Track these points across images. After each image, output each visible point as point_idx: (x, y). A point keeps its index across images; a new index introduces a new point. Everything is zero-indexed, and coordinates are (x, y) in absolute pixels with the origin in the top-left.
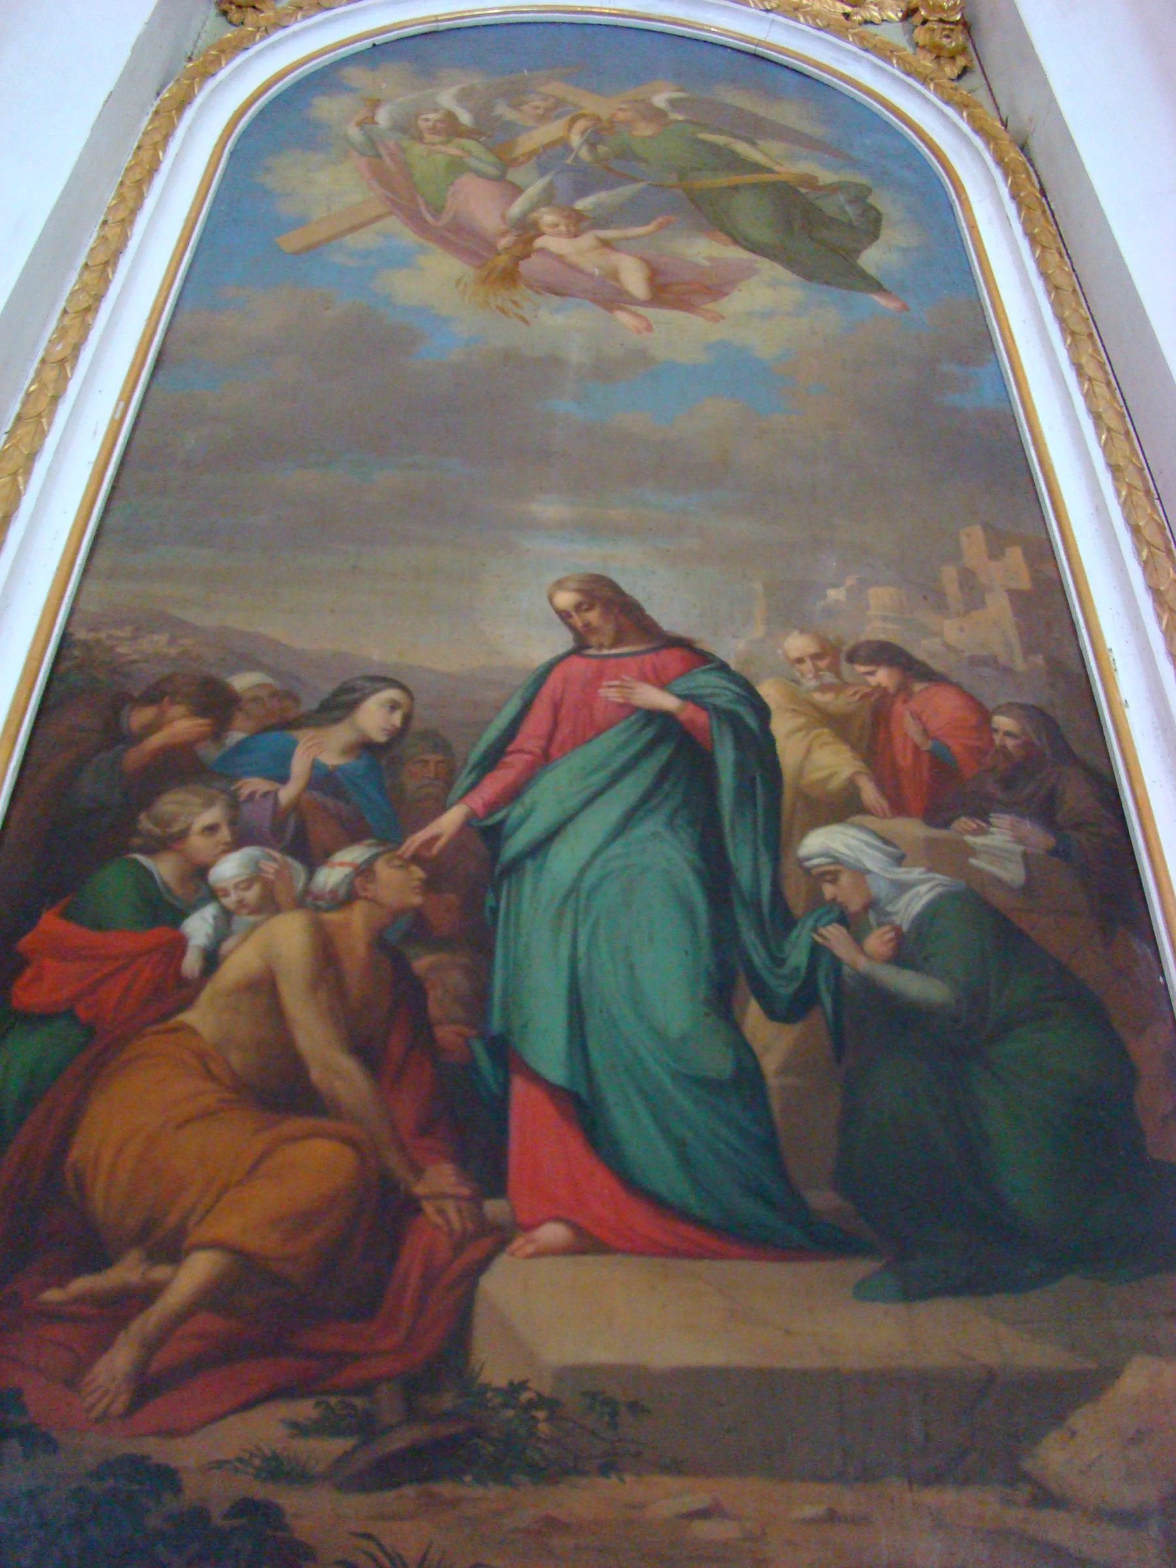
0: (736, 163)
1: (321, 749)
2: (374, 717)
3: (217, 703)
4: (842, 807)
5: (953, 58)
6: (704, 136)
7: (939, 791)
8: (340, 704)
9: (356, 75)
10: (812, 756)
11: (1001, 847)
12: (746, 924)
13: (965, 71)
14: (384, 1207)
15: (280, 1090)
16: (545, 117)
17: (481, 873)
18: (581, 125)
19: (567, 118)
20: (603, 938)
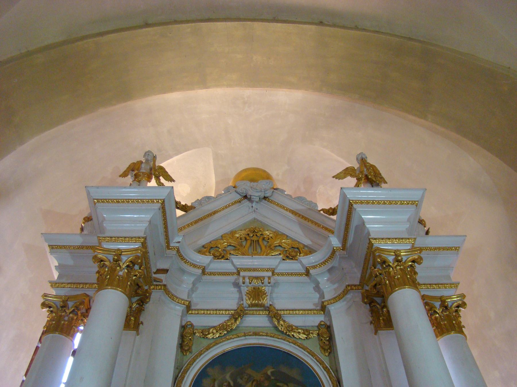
5: (327, 350)
6: (278, 384)
9: (209, 370)
13: (330, 353)
16: (247, 382)
18: (254, 383)
19: (251, 382)
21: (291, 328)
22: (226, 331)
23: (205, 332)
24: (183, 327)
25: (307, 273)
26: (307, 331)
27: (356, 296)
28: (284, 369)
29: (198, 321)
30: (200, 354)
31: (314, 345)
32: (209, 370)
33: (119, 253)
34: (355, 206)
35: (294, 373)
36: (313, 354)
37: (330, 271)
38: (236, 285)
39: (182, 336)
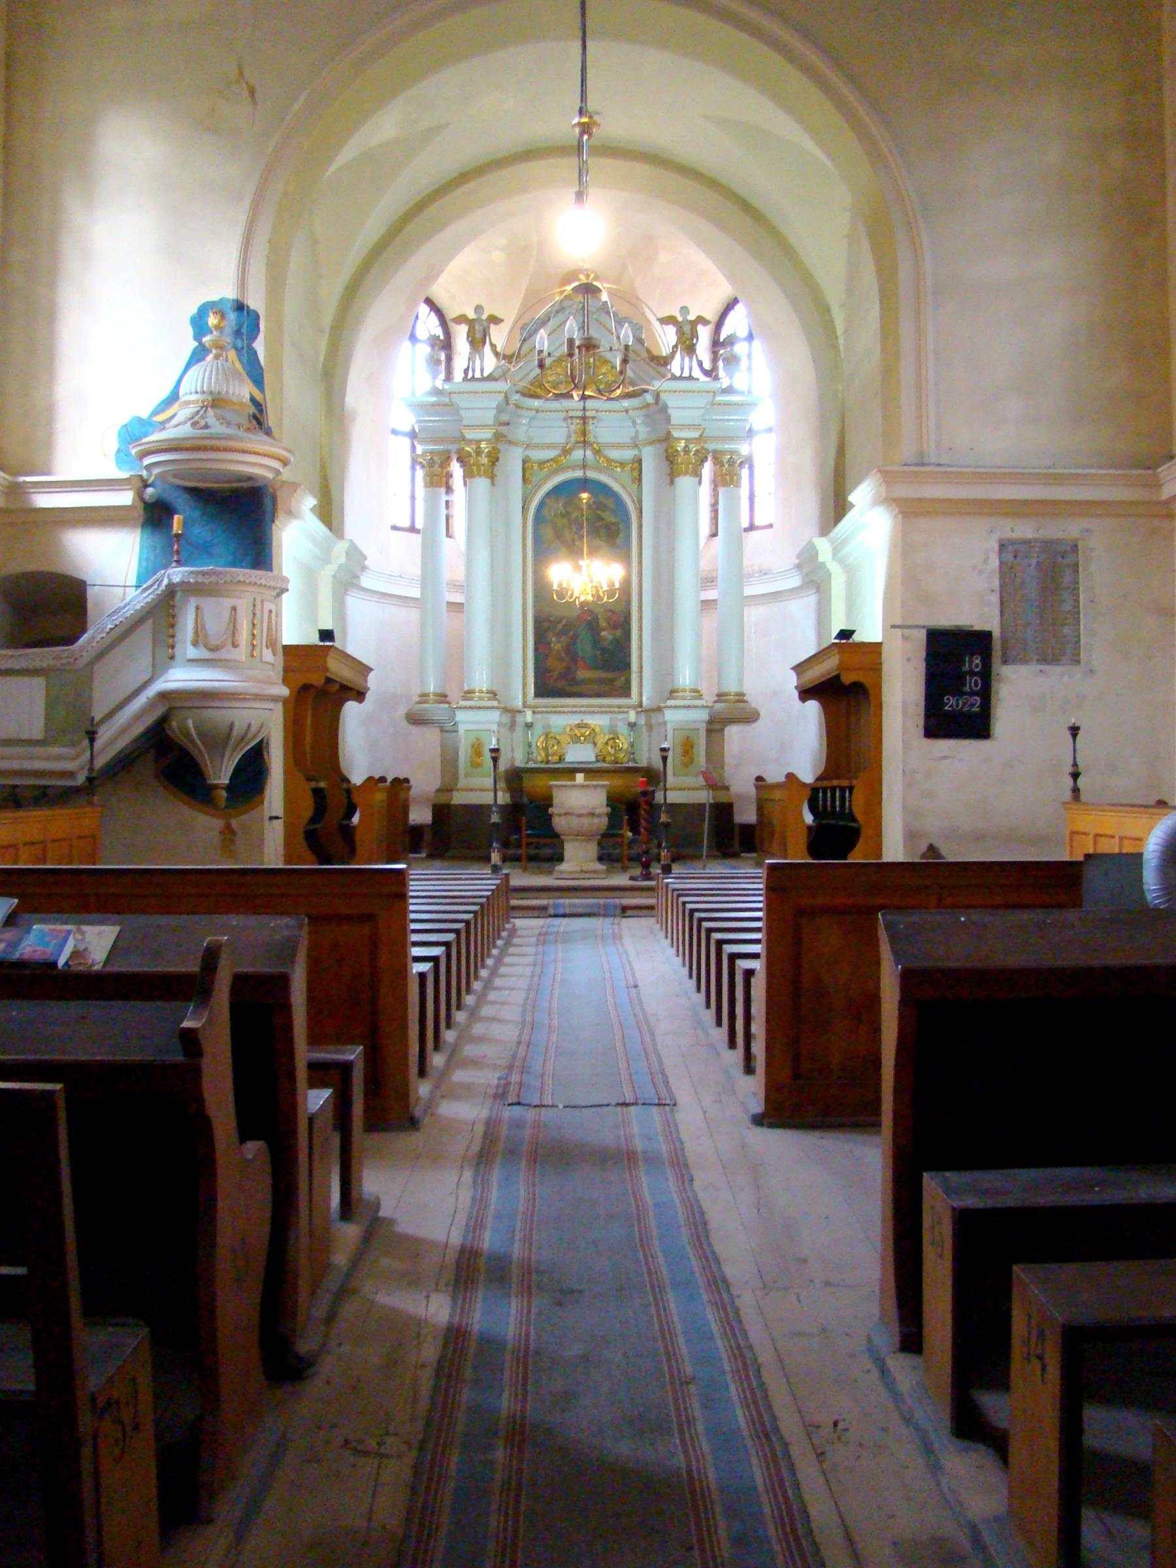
0: (602, 519)
1: (559, 626)
2: (564, 622)
3: (550, 621)
4: (604, 630)
7: (614, 626)
8: (560, 621)
9: (547, 501)
10: (603, 624)
11: (619, 633)
12: (596, 641)
14: (568, 668)
15: (561, 660)
17: (575, 638)
20: (585, 647)
21: (609, 461)
22: (556, 465)
23: (541, 464)
24: (524, 462)
25: (627, 411)
26: (622, 465)
27: (661, 447)
28: (602, 499)
29: (537, 455)
30: (539, 487)
31: (626, 476)
32: (547, 501)
33: (479, 441)
34: (662, 395)
35: (610, 503)
36: (624, 487)
37: (646, 416)
38: (565, 419)
39: (524, 469)
